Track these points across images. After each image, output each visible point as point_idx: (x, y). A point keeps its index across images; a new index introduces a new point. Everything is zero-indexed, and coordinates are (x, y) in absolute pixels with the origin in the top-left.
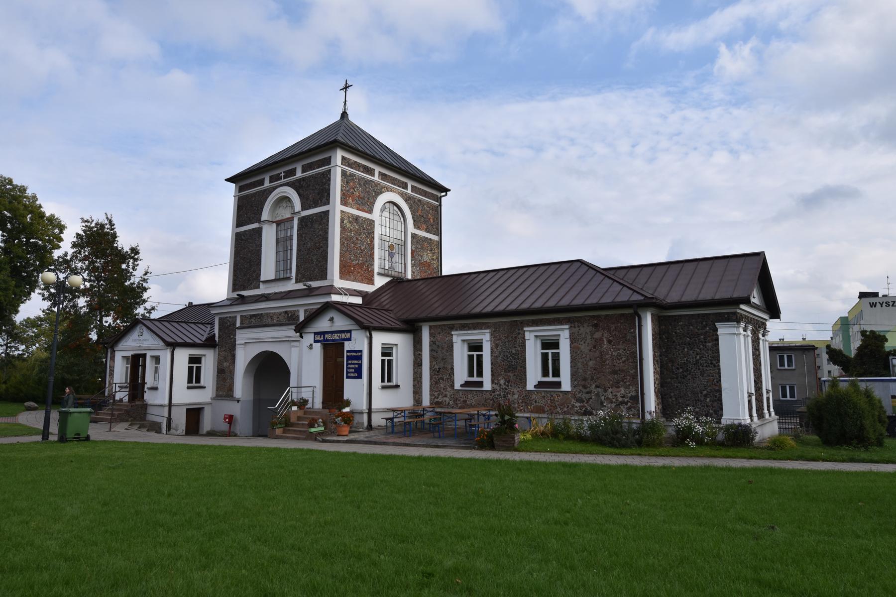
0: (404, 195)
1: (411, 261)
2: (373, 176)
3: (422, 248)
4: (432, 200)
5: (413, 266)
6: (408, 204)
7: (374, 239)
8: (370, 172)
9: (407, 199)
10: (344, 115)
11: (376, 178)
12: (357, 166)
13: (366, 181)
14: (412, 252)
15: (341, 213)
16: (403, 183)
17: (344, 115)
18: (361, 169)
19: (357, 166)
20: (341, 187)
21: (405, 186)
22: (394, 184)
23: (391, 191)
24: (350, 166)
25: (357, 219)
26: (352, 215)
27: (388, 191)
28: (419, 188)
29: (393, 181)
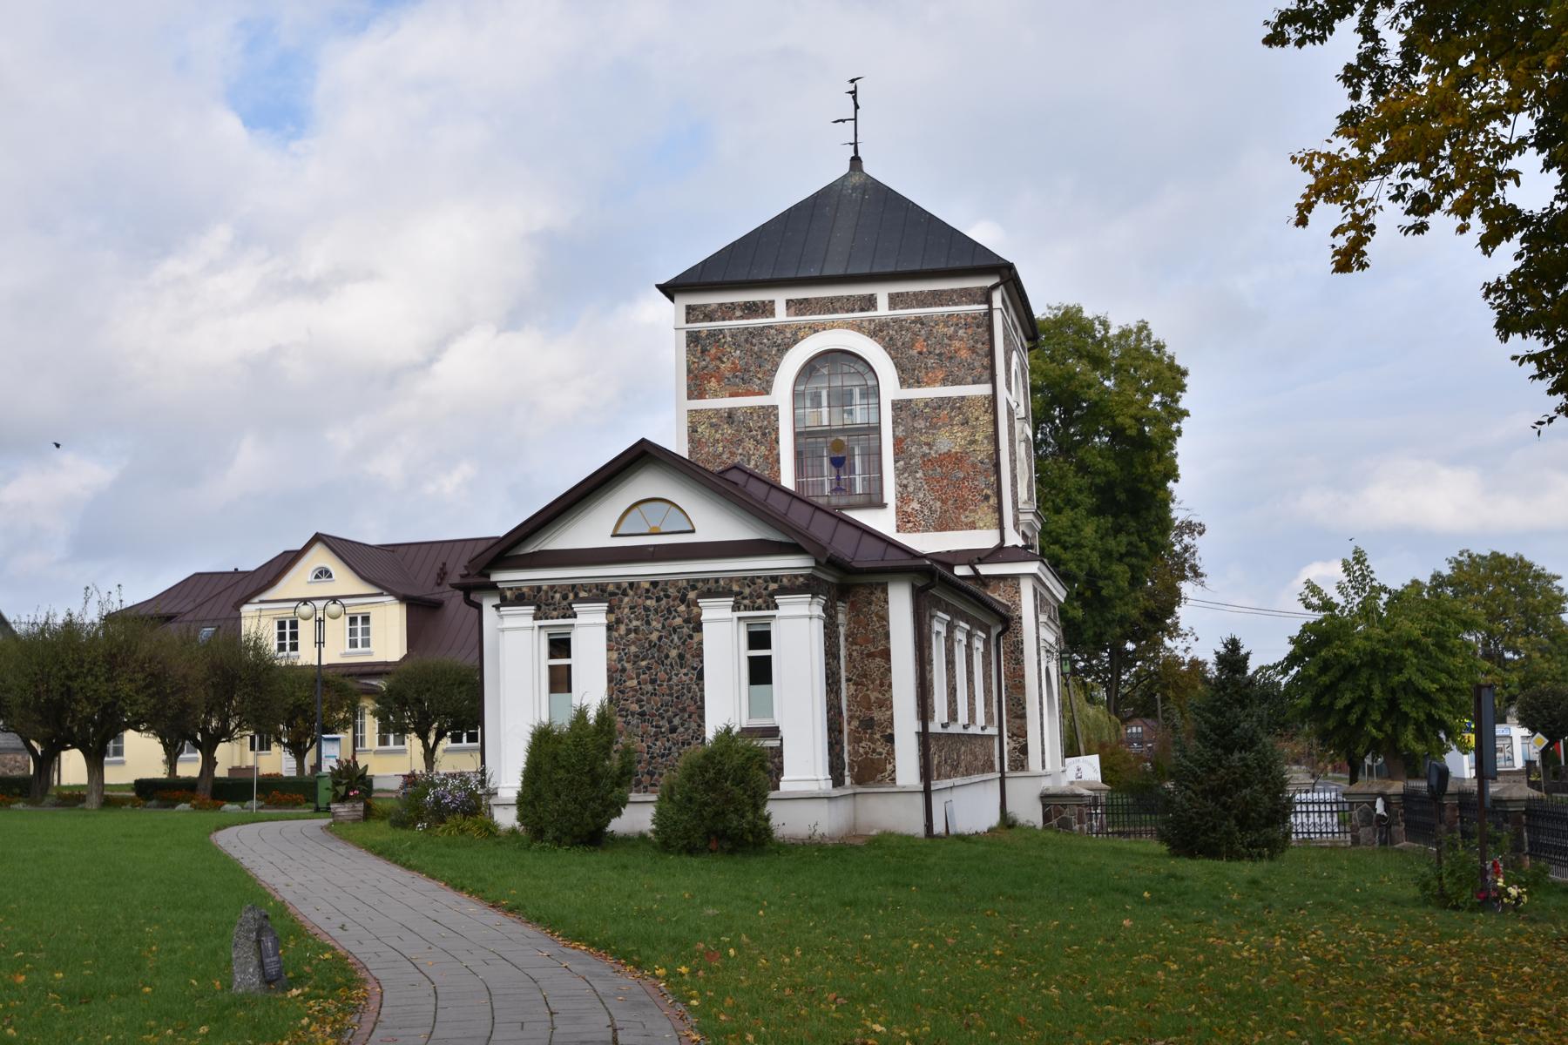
0: (866, 324)
1: (896, 461)
2: (772, 314)
3: (933, 426)
4: (967, 304)
5: (899, 473)
6: (881, 341)
7: (778, 442)
8: (766, 309)
9: (877, 331)
10: (856, 161)
11: (781, 316)
12: (727, 311)
13: (750, 333)
14: (898, 442)
15: (689, 416)
16: (862, 298)
17: (856, 161)
18: (738, 313)
19: (727, 311)
20: (688, 367)
21: (870, 302)
22: (835, 311)
23: (824, 329)
24: (709, 317)
25: (730, 415)
26: (717, 411)
27: (816, 331)
28: (915, 294)
29: (831, 306)
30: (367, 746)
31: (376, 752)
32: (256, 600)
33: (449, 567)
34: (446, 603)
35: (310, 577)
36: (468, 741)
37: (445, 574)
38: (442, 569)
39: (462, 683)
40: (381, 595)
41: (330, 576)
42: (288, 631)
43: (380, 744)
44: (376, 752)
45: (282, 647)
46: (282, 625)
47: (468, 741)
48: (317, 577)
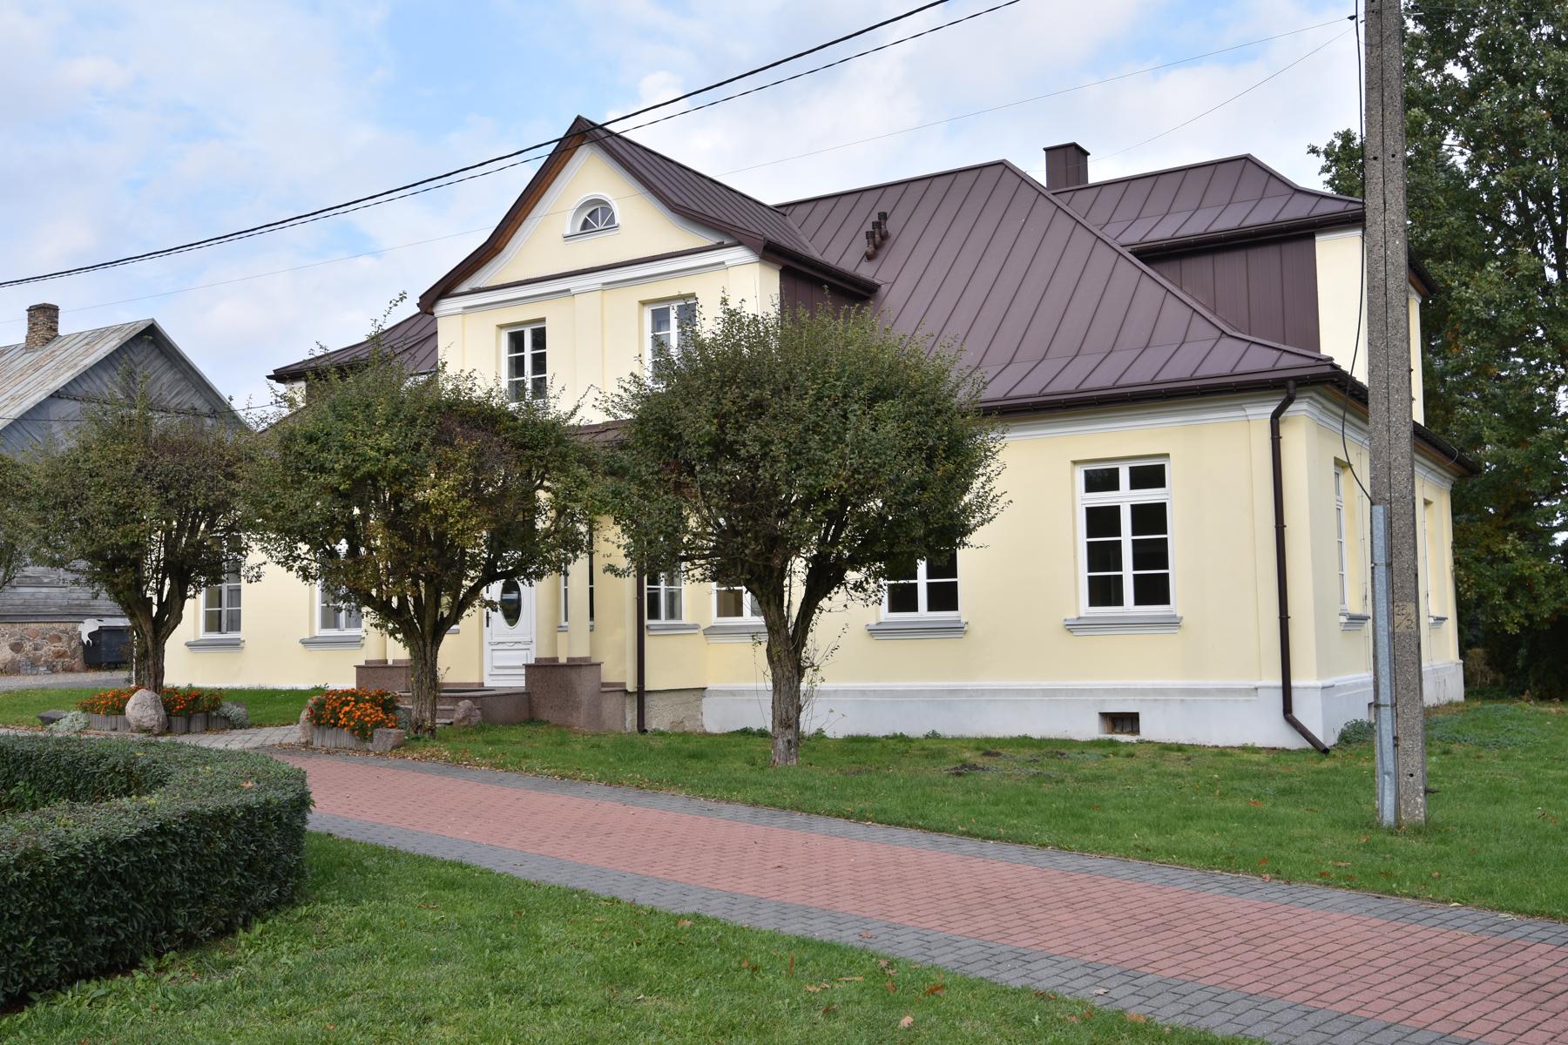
30: (687, 617)
31: (711, 631)
32: (464, 287)
33: (891, 226)
34: (884, 289)
35: (569, 224)
36: (931, 608)
37: (885, 237)
38: (877, 225)
39: (879, 395)
40: (720, 246)
41: (612, 220)
42: (528, 353)
43: (719, 615)
44: (711, 631)
45: (517, 390)
46: (516, 341)
47: (931, 608)
48: (585, 225)
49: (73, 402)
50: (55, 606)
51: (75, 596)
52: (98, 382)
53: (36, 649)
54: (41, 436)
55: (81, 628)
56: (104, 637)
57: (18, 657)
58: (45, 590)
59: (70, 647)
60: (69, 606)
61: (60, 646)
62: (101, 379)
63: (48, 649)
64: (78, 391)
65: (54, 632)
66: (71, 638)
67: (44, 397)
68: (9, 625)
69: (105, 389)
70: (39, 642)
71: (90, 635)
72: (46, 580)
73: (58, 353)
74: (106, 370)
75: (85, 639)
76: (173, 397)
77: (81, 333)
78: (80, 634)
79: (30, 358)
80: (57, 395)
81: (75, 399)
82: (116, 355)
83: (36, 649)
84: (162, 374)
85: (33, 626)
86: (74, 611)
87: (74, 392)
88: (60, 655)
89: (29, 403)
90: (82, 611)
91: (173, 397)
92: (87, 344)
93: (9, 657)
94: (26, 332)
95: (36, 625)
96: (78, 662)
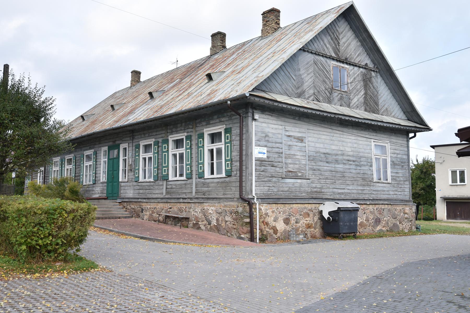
49: (310, 55)
50: (305, 192)
51: (314, 185)
52: (322, 43)
53: (296, 223)
54: (295, 76)
55: (321, 208)
56: (342, 215)
57: (288, 228)
58: (299, 181)
59: (314, 221)
60: (312, 192)
61: (309, 220)
62: (323, 41)
63: (303, 222)
64: (312, 48)
65: (305, 211)
66: (314, 215)
67: (296, 51)
68: (283, 205)
69: (325, 48)
70: (298, 217)
71: (330, 213)
72: (300, 174)
73: (288, 32)
74: (325, 35)
75: (326, 215)
76: (357, 57)
77: (296, 23)
78: (321, 212)
79: (266, 41)
80: (303, 50)
81: (311, 53)
82: (337, 21)
83: (296, 223)
84: (352, 41)
85: (295, 206)
86: (314, 196)
87: (310, 48)
88: (309, 226)
89: (286, 56)
90: (318, 196)
91: (357, 57)
92: (307, 23)
93: (283, 228)
94: (261, 27)
95: (296, 205)
96: (318, 231)
